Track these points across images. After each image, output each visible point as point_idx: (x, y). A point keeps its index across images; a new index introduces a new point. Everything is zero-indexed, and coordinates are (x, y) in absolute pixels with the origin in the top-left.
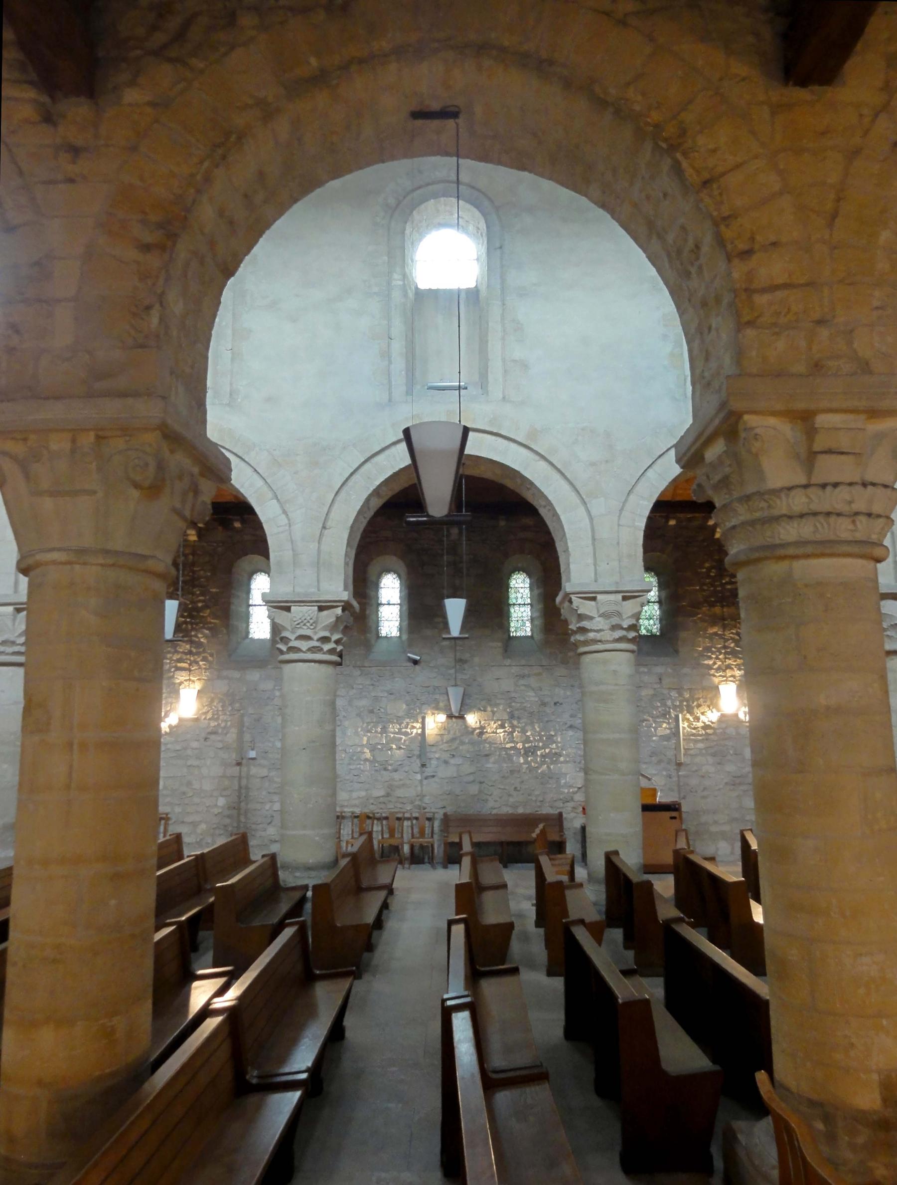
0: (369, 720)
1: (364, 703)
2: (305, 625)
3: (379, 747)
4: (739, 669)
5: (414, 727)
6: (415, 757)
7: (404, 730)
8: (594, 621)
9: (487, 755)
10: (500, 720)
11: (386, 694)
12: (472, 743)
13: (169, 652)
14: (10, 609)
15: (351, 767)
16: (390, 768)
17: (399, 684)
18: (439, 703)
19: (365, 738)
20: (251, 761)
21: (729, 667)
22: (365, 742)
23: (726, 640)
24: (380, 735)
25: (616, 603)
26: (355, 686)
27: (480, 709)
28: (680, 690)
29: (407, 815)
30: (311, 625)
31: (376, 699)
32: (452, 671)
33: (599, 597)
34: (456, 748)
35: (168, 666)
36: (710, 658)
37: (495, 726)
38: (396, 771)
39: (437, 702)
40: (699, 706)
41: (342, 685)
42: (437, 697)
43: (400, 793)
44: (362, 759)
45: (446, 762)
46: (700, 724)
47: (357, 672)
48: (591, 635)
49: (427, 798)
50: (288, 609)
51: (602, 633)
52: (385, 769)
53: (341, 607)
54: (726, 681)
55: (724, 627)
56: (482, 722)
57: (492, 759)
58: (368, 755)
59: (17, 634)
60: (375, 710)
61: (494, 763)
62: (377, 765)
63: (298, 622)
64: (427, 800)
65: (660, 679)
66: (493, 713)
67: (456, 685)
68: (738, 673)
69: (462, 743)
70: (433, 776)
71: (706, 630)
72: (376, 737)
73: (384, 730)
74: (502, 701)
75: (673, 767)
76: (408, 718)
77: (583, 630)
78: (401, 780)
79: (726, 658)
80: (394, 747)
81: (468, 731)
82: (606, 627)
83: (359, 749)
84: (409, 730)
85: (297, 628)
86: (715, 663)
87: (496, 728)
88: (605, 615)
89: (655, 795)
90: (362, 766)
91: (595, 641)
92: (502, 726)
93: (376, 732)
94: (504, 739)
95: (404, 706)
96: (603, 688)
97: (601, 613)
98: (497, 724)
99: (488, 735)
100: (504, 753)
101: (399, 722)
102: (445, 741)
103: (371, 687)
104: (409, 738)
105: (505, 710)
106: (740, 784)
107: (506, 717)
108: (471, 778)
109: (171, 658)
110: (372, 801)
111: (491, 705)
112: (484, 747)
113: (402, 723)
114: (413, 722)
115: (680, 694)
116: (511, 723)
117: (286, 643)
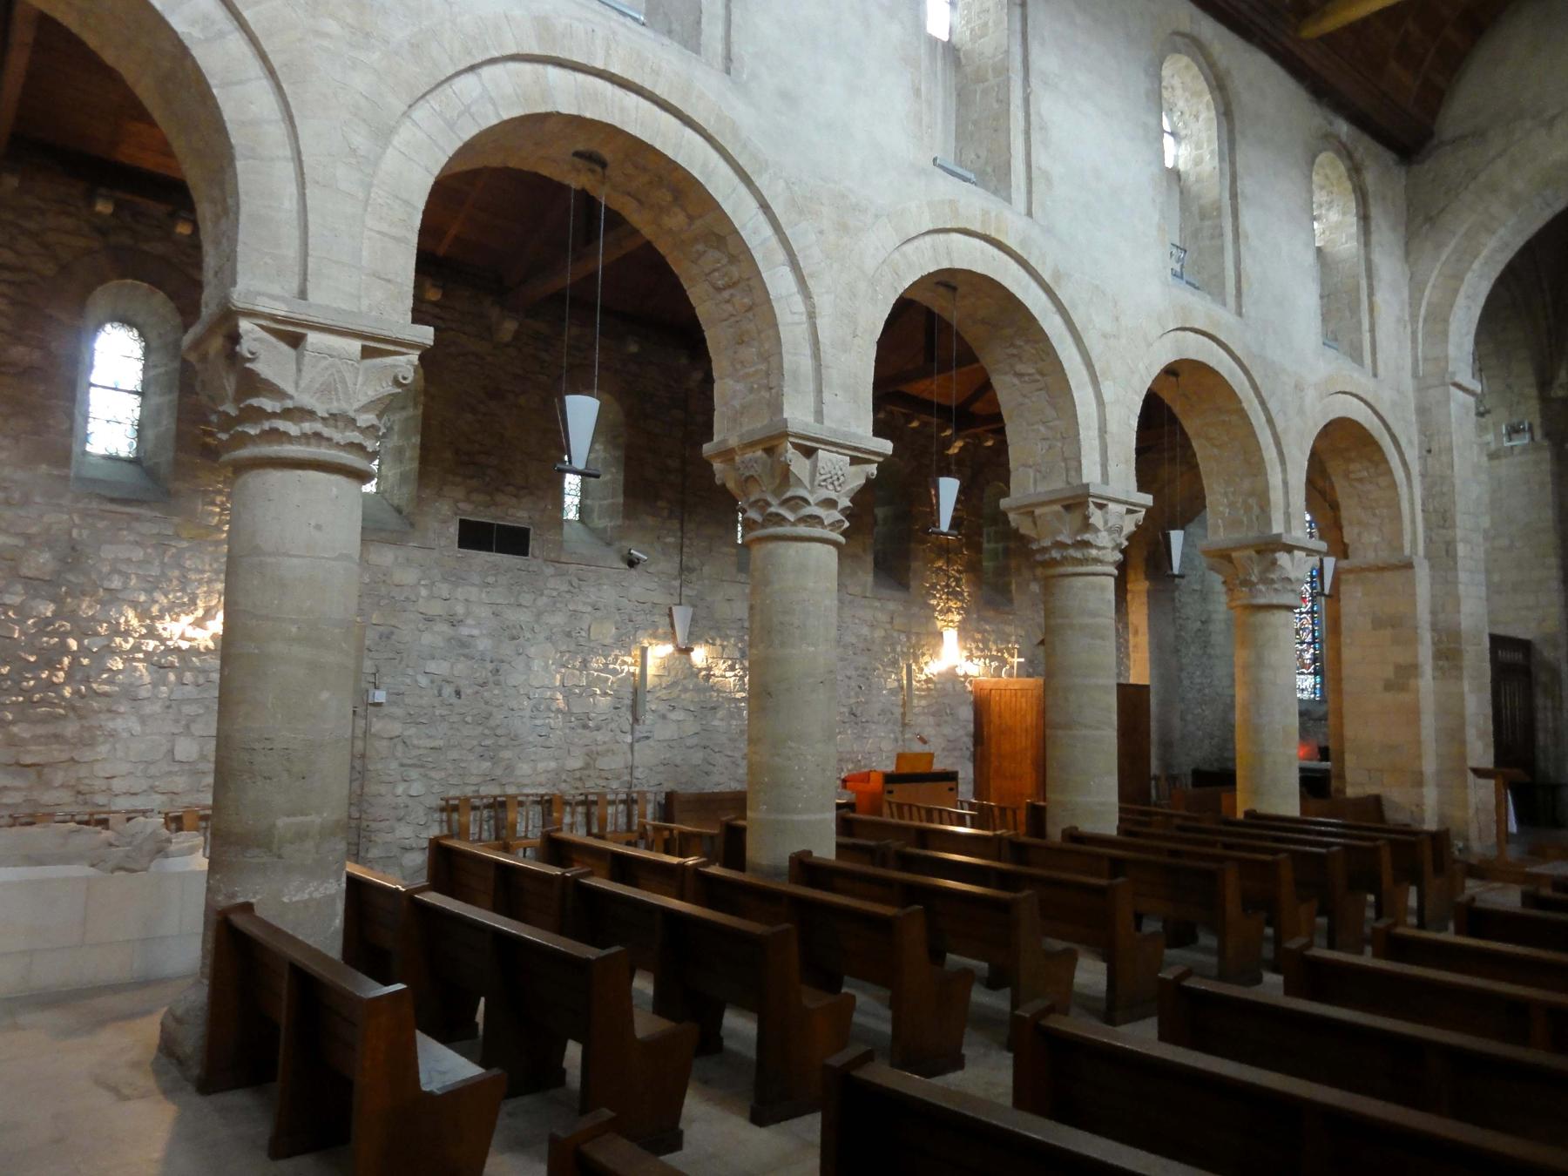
0: (564, 648)
1: (558, 619)
2: (832, 483)
3: (577, 691)
4: (959, 614)
5: (624, 663)
6: (624, 709)
7: (611, 666)
8: (1099, 534)
9: (714, 708)
10: (731, 659)
11: (589, 609)
12: (698, 690)
13: (220, 492)
14: (356, 346)
15: (538, 722)
16: (591, 724)
17: (608, 595)
18: (657, 628)
19: (558, 676)
20: (371, 709)
21: (949, 610)
22: (558, 684)
23: (949, 578)
24: (578, 672)
25: (1121, 517)
26: (546, 592)
27: (707, 642)
28: (908, 634)
29: (610, 797)
30: (840, 485)
31: (575, 614)
32: (676, 583)
33: (1111, 506)
34: (679, 696)
35: (217, 518)
36: (935, 597)
37: (724, 667)
38: (598, 729)
39: (654, 625)
40: (923, 654)
41: (525, 588)
42: (656, 618)
43: (602, 763)
44: (554, 709)
45: (664, 717)
46: (923, 677)
47: (549, 570)
48: (1094, 552)
49: (640, 770)
50: (809, 452)
51: (1104, 552)
52: (585, 727)
53: (876, 465)
54: (947, 626)
55: (948, 562)
56: (710, 661)
57: (720, 714)
58: (561, 703)
59: (356, 405)
60: (574, 634)
61: (722, 720)
62: (573, 719)
63: (824, 477)
64: (637, 774)
65: (892, 618)
66: (724, 647)
67: (680, 604)
68: (957, 618)
69: (685, 690)
70: (647, 738)
71: (933, 562)
72: (573, 675)
73: (585, 663)
74: (734, 633)
75: (898, 729)
76: (617, 648)
77: (1087, 544)
78: (605, 743)
79: (948, 599)
80: (598, 692)
81: (693, 672)
82: (1110, 545)
83: (549, 694)
84: (618, 667)
85: (820, 485)
86: (938, 604)
87: (725, 670)
88: (1110, 531)
89: (931, 762)
90: (551, 721)
91: (1097, 561)
92: (732, 668)
93: (574, 667)
94: (735, 685)
95: (614, 630)
96: (1099, 620)
97: (1109, 525)
98: (726, 664)
99: (717, 679)
100: (733, 705)
101: (606, 653)
102: (664, 686)
103: (568, 596)
104: (619, 679)
105: (735, 645)
106: (954, 749)
107: (737, 655)
108: (695, 741)
109: (223, 503)
110: (564, 777)
111: (720, 637)
112: (711, 696)
113: (610, 655)
114: (624, 656)
115: (909, 639)
116: (741, 663)
117: (793, 510)
